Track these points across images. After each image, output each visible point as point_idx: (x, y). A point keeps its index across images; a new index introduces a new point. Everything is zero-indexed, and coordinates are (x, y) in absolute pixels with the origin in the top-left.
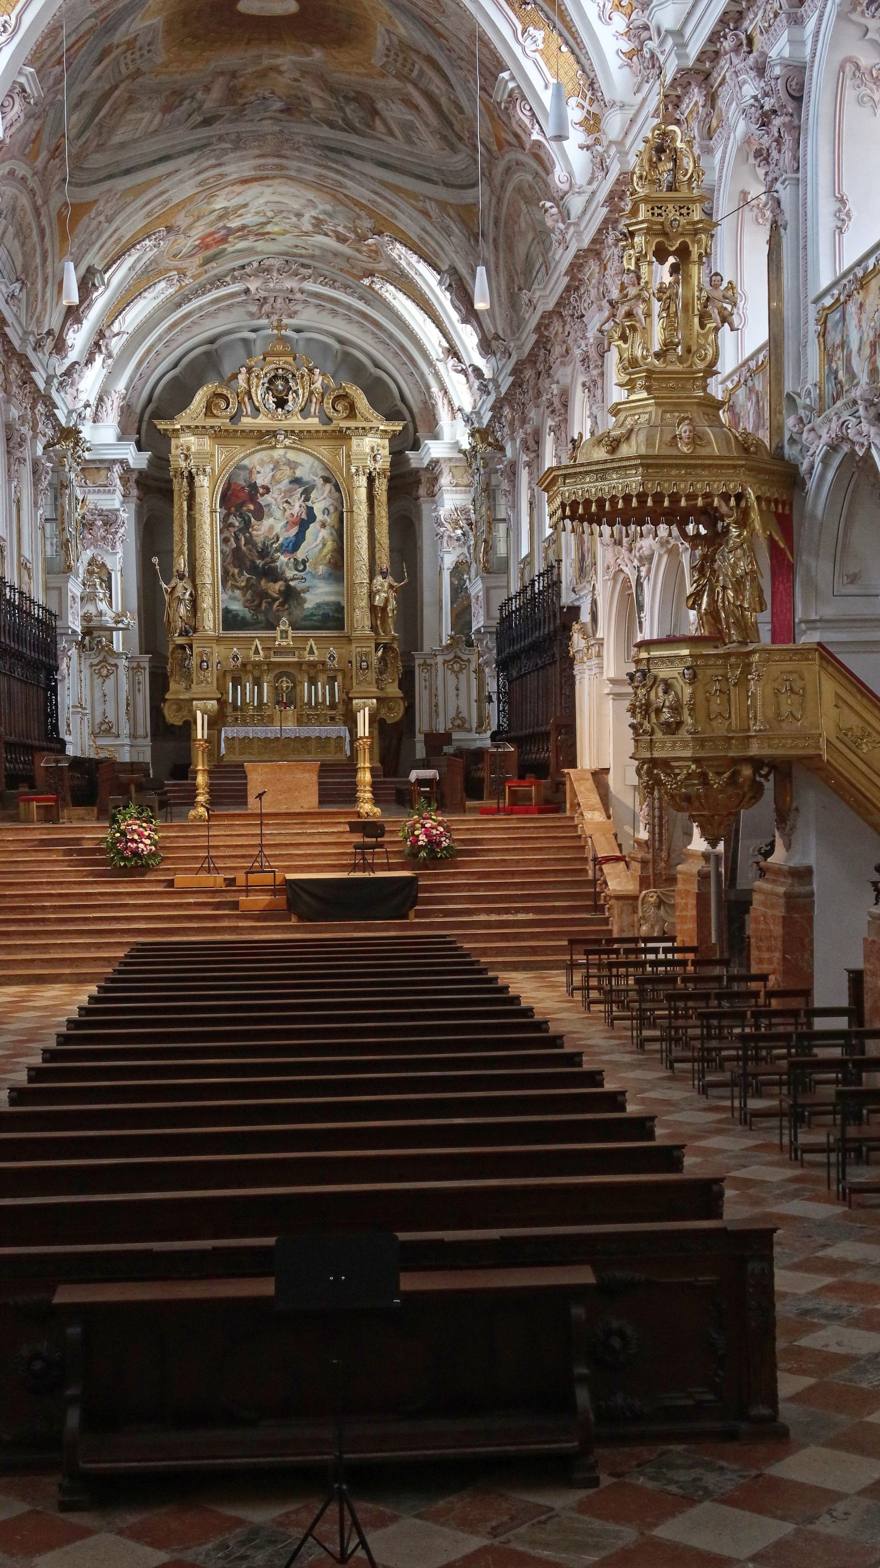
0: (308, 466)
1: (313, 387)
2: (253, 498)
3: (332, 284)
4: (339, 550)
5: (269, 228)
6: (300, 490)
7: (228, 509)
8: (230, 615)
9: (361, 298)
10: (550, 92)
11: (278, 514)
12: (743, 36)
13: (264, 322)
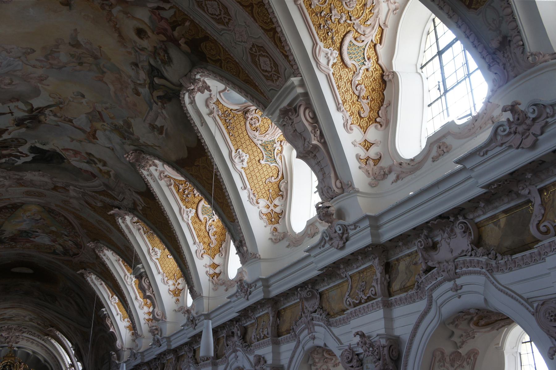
3: (34, 335)
5: (13, 319)
9: (43, 340)
10: (119, 316)
12: (192, 349)
13: (6, 345)
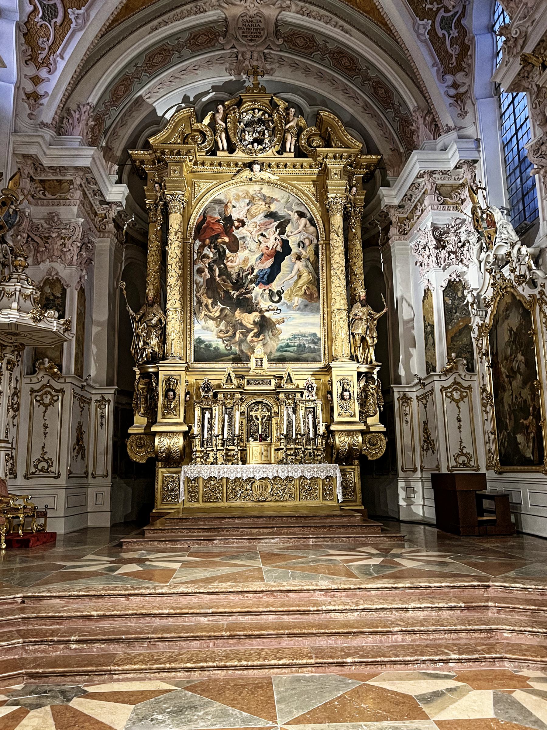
0: (283, 201)
1: (287, 126)
2: (228, 232)
4: (316, 282)
6: (276, 224)
7: (203, 241)
8: (203, 346)
11: (253, 246)
